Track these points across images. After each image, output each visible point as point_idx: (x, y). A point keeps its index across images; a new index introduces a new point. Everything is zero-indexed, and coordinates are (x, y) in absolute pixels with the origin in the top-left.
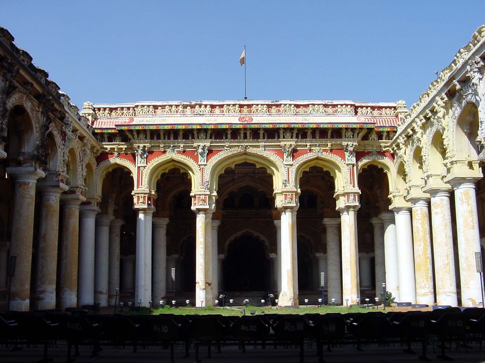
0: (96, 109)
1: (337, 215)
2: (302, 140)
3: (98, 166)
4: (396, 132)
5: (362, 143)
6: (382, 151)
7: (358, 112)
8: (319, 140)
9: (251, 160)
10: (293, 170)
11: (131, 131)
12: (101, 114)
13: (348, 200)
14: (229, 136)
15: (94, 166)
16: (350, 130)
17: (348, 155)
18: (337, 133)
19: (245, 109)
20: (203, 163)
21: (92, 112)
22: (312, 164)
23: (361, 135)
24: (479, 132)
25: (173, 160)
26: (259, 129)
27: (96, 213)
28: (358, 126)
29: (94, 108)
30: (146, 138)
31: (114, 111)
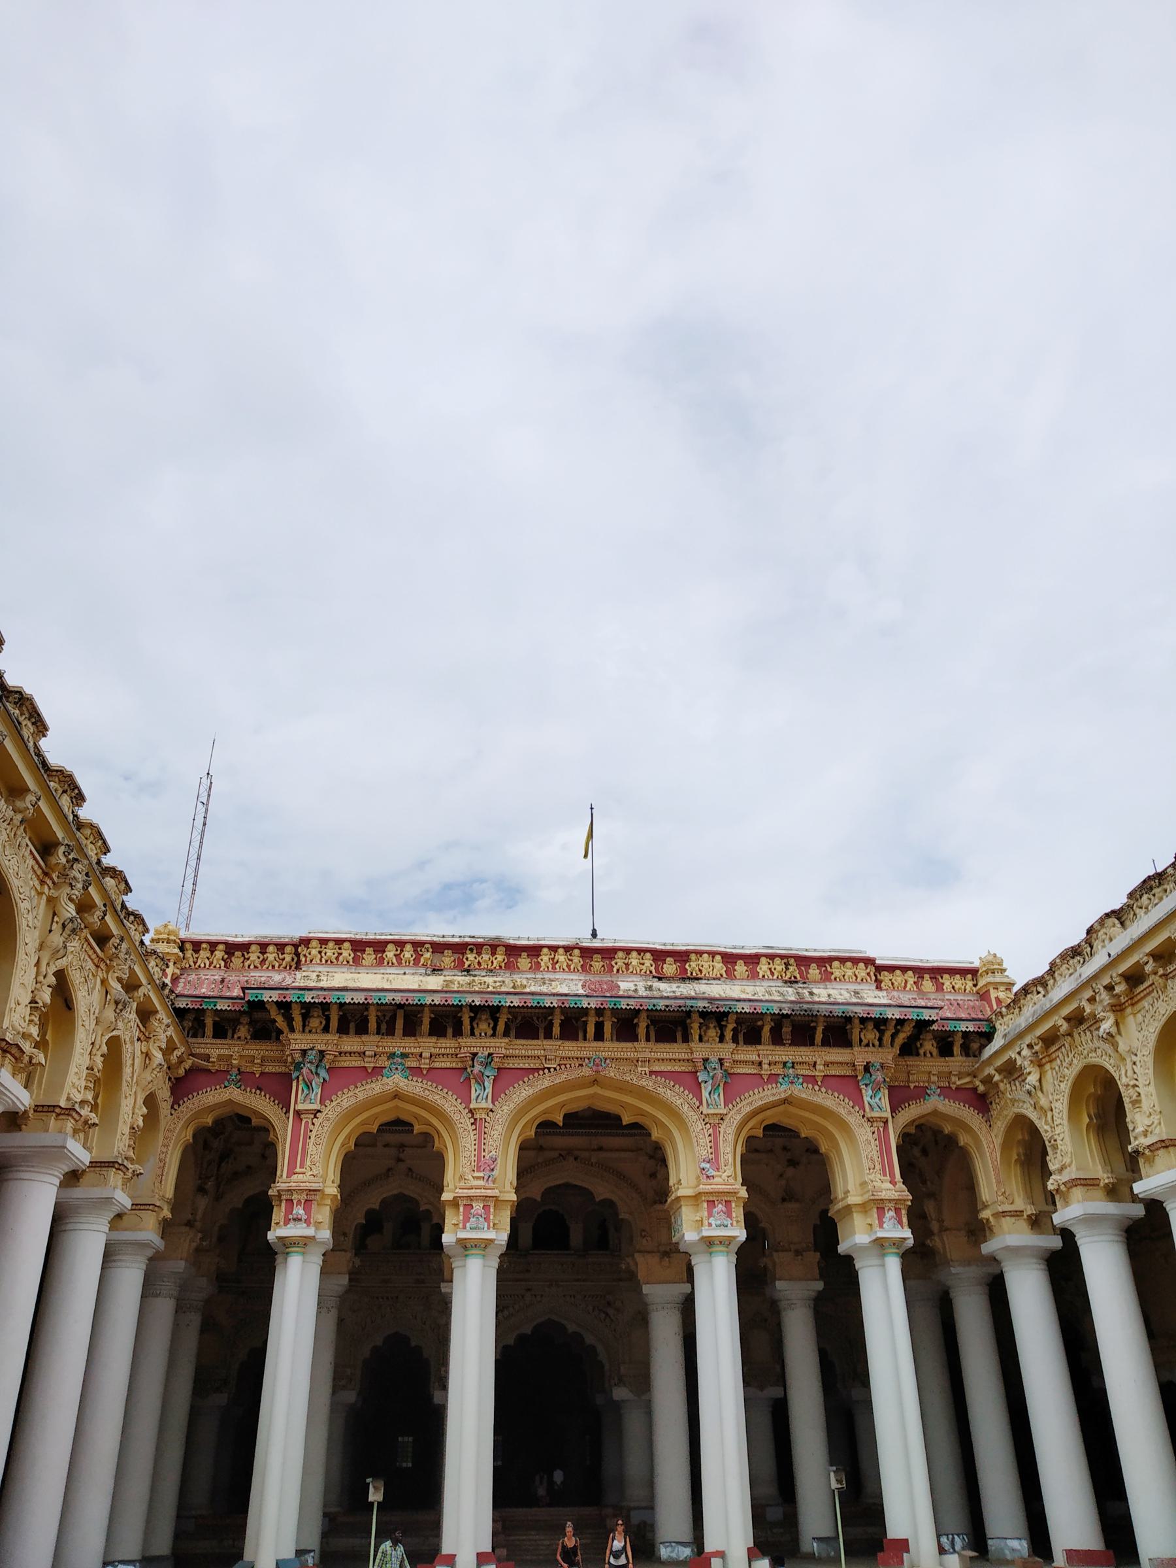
0: (188, 946)
2: (750, 1048)
3: (176, 1107)
4: (988, 1036)
5: (901, 1062)
6: (954, 1087)
7: (881, 982)
8: (794, 1048)
9: (607, 1099)
10: (728, 1131)
11: (284, 1007)
12: (199, 961)
14: (556, 1030)
15: (164, 1108)
16: (870, 1026)
17: (870, 1092)
18: (839, 1030)
19: (597, 963)
20: (484, 1105)
21: (177, 950)
22: (771, 1117)
23: (901, 1037)
25: (396, 1096)
26: (637, 1012)
27: (150, 1253)
28: (896, 1014)
29: (183, 942)
30: (326, 1029)
31: (238, 954)
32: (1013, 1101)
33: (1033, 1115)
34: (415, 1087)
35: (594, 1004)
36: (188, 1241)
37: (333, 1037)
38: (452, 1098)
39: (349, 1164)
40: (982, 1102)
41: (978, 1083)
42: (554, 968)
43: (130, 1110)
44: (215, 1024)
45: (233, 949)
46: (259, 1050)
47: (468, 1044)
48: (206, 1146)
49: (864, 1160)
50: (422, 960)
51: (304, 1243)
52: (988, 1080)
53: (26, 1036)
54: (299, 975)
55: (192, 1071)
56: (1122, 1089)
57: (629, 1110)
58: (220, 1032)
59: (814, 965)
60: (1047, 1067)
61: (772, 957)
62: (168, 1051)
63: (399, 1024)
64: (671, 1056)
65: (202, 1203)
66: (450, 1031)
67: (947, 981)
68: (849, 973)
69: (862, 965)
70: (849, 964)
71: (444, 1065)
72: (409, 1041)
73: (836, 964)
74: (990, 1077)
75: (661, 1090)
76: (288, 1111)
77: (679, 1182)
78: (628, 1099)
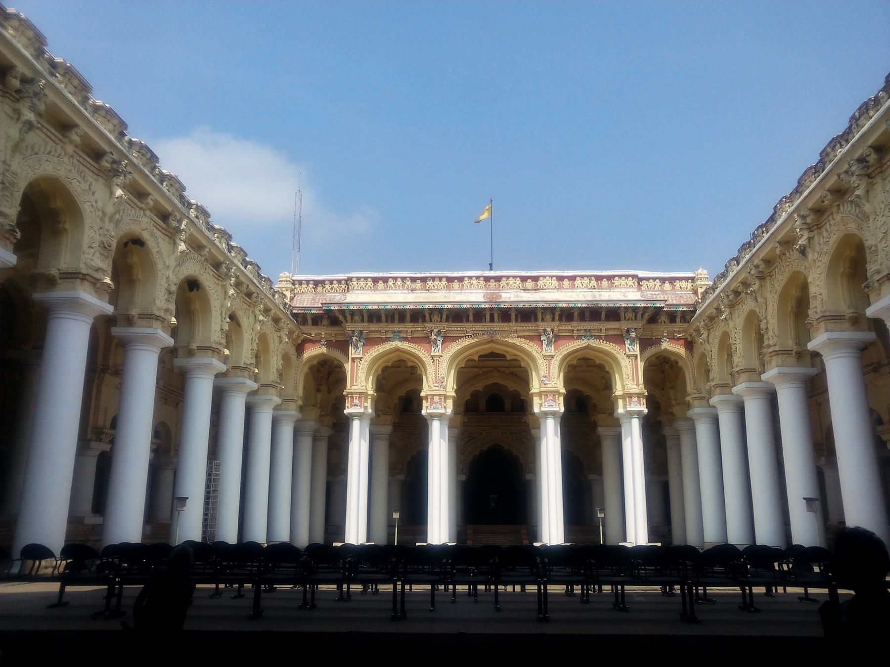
1: (616, 424)
4: (694, 312)
9: (498, 349)
10: (556, 363)
11: (342, 312)
14: (471, 318)
18: (613, 313)
21: (291, 285)
22: (581, 354)
23: (646, 316)
24: (810, 312)
25: (398, 350)
26: (510, 309)
27: (295, 419)
30: (362, 321)
36: (314, 413)
37: (365, 324)
41: (687, 336)
43: (275, 362)
46: (333, 330)
48: (319, 371)
51: (360, 416)
52: (691, 335)
53: (220, 344)
54: (348, 295)
57: (510, 354)
62: (291, 333)
63: (397, 317)
65: (319, 396)
66: (420, 320)
67: (678, 284)
68: (623, 283)
72: (401, 325)
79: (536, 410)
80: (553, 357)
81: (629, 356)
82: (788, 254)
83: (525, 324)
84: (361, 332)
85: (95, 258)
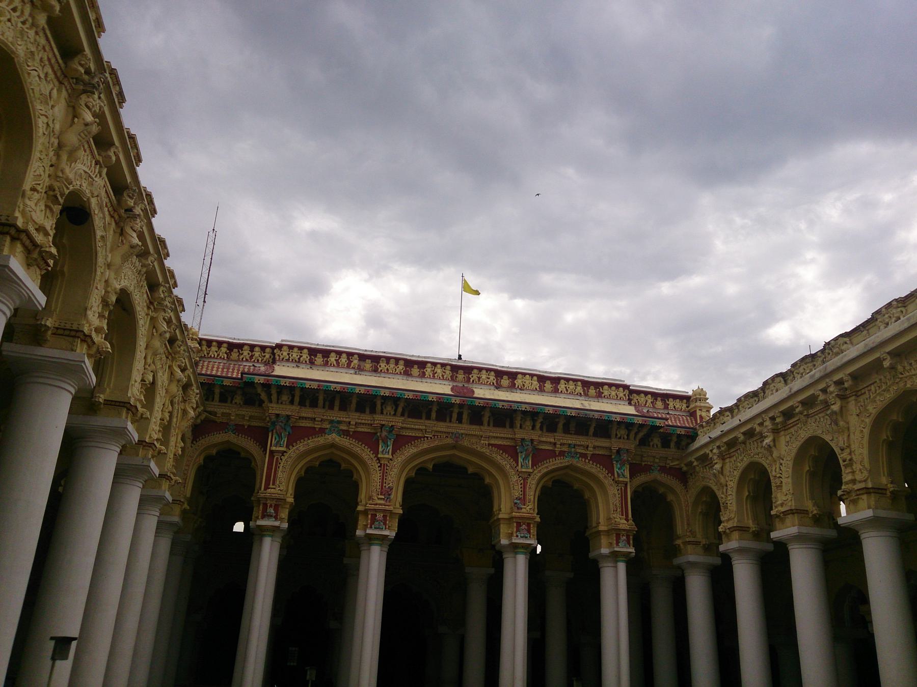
0: (204, 343)
10: (532, 482)
11: (267, 386)
13: (617, 544)
14: (434, 415)
19: (461, 376)
20: (386, 456)
23: (641, 435)
25: (332, 445)
26: (483, 408)
28: (640, 421)
29: (201, 340)
30: (292, 402)
32: (704, 478)
33: (715, 488)
34: (345, 442)
35: (457, 400)
37: (295, 408)
38: (367, 450)
39: (300, 484)
40: (683, 476)
42: (434, 376)
43: (175, 444)
44: (221, 394)
45: (232, 346)
46: (248, 412)
47: (379, 419)
49: (611, 506)
50: (352, 365)
55: (206, 421)
56: (772, 478)
58: (223, 399)
59: (592, 387)
60: (727, 460)
61: (567, 380)
63: (337, 403)
64: (502, 435)
66: (368, 410)
67: (671, 403)
68: (613, 393)
69: (621, 389)
70: (614, 388)
71: (363, 430)
72: (343, 414)
73: (606, 387)
74: (691, 463)
75: (494, 455)
76: (265, 450)
77: (500, 510)
78: (474, 459)
79: (504, 541)
80: (529, 474)
81: (617, 482)
82: (900, 368)
83: (500, 429)
84: (288, 417)
85: (38, 209)
